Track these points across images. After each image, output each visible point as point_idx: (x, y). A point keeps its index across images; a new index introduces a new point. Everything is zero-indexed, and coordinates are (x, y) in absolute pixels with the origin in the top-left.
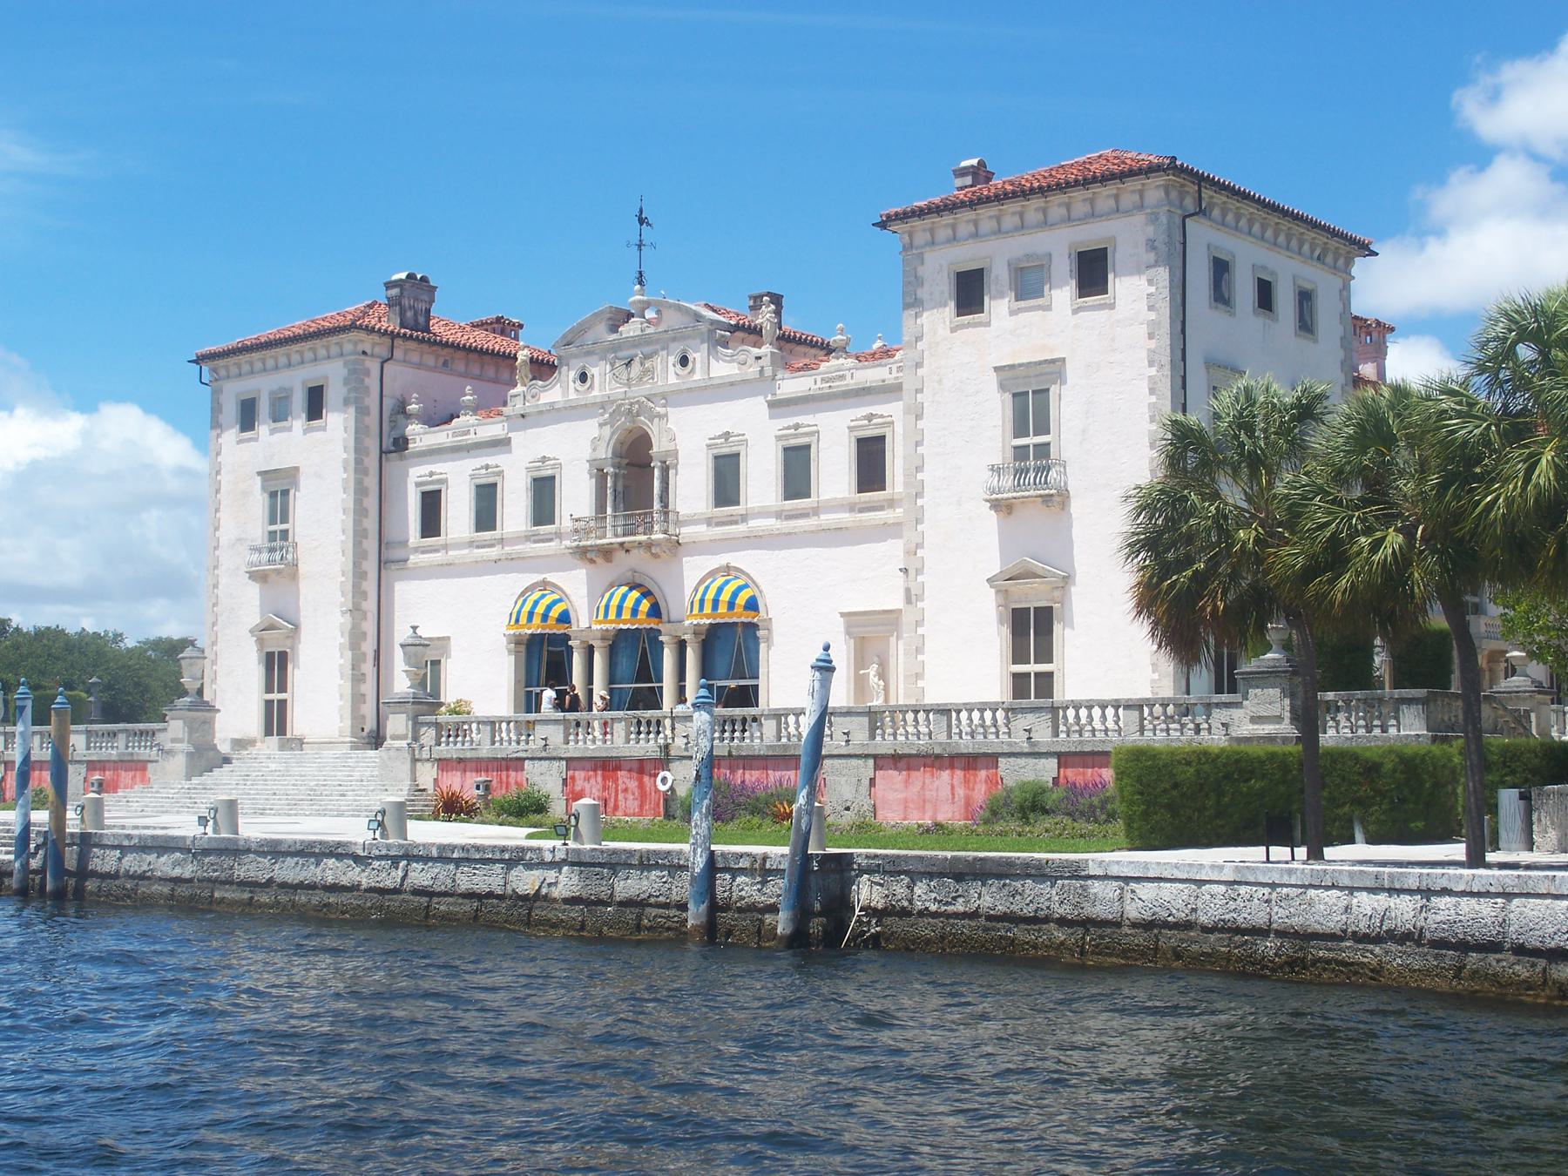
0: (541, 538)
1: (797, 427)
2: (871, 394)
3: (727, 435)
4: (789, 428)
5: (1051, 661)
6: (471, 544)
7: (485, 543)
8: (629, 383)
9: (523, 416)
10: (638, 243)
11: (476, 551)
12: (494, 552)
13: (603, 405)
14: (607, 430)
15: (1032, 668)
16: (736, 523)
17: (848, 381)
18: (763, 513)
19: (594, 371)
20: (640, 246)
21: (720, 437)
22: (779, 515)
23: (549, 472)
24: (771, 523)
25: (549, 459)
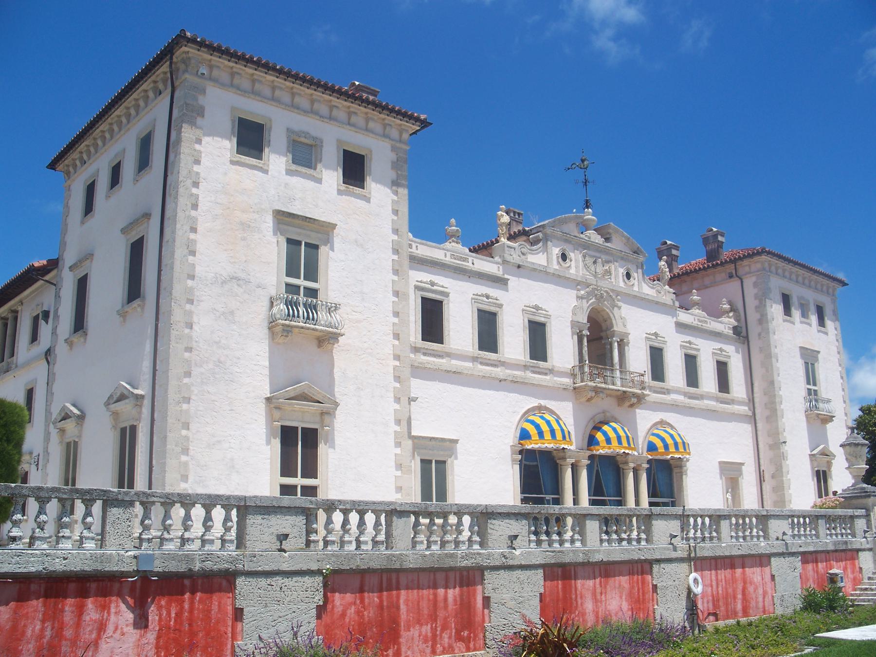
0: (537, 370)
1: (690, 342)
2: (721, 337)
3: (656, 334)
4: (686, 342)
5: (301, 477)
6: (474, 359)
7: (489, 362)
8: (595, 275)
9: (519, 267)
10: (588, 184)
11: (480, 367)
12: (499, 372)
13: (579, 283)
14: (585, 304)
15: (299, 481)
16: (664, 393)
17: (708, 325)
18: (677, 391)
19: (572, 255)
20: (586, 183)
21: (652, 335)
22: (685, 394)
23: (542, 320)
24: (680, 398)
25: (541, 309)
